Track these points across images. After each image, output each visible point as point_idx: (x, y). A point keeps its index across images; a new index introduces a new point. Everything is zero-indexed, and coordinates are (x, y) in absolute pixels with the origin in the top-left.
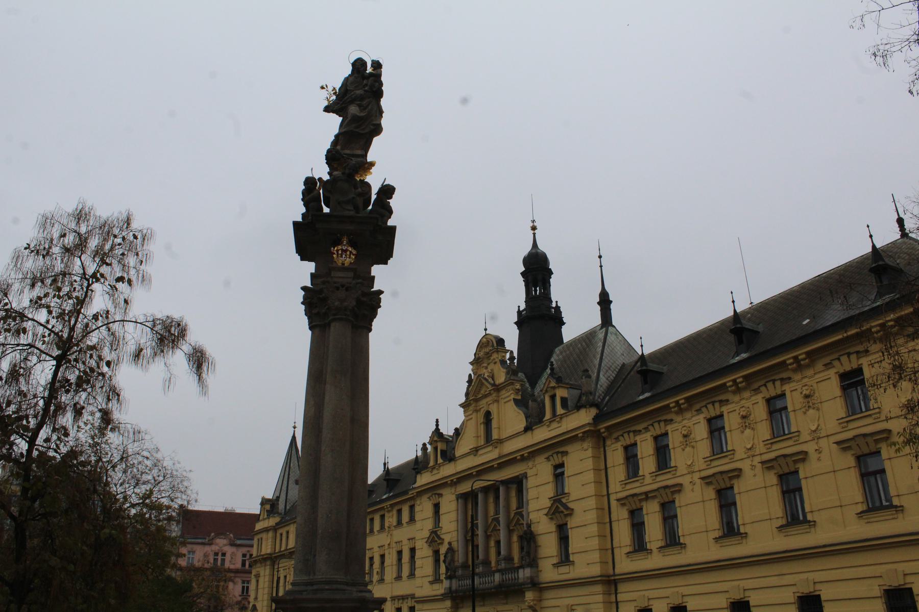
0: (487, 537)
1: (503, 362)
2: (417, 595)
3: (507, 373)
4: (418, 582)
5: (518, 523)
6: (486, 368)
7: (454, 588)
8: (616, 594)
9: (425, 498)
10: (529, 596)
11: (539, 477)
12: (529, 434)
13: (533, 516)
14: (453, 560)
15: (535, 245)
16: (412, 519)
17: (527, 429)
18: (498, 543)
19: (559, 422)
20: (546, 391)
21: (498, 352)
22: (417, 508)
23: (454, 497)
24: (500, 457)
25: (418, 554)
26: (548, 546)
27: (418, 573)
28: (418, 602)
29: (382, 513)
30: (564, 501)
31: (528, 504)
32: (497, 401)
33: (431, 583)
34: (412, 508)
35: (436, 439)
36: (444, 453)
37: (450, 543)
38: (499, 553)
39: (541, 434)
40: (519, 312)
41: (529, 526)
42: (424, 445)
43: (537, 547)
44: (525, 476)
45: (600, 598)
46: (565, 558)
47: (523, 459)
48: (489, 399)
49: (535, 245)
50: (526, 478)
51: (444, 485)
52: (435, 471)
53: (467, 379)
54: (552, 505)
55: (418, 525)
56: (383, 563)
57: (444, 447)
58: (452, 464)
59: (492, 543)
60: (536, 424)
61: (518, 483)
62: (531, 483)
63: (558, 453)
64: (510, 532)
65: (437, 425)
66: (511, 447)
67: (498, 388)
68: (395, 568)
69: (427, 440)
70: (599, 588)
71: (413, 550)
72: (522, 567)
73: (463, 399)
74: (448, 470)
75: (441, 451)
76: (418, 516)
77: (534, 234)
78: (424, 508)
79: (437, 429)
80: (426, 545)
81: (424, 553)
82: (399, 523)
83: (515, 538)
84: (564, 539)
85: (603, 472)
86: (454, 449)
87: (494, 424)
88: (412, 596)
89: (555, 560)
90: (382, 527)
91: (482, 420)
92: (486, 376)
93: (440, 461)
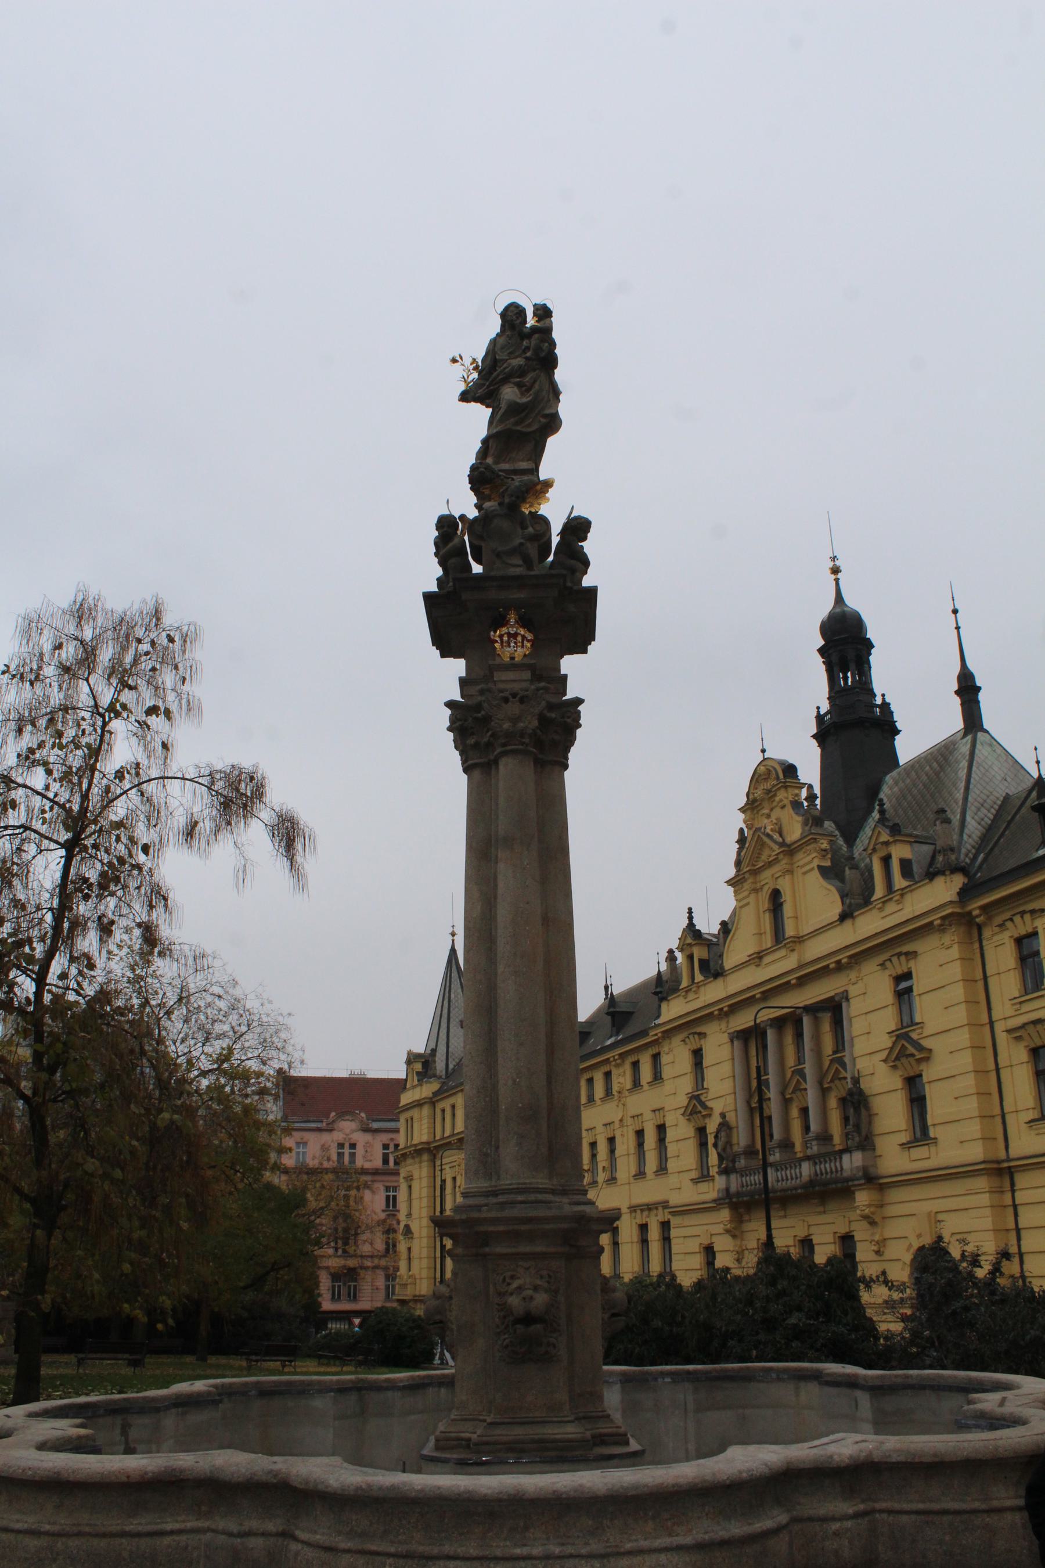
0: (786, 1102)
1: (796, 805)
2: (672, 1203)
3: (805, 823)
4: (672, 1180)
5: (836, 1077)
6: (768, 816)
8: (1013, 1191)
10: (863, 1198)
13: (862, 1064)
14: (729, 1143)
16: (657, 1077)
17: (844, 917)
18: (805, 1111)
21: (786, 787)
22: (665, 1059)
24: (801, 967)
25: (671, 1135)
27: (671, 1165)
29: (606, 1068)
31: (852, 1046)
32: (790, 872)
33: (695, 1181)
34: (656, 1057)
35: (689, 941)
36: (704, 965)
38: (807, 1128)
41: (856, 1081)
42: (671, 952)
43: (871, 1116)
44: (845, 996)
45: (985, 1199)
46: (921, 1133)
48: (776, 869)
50: (847, 999)
51: (709, 1017)
52: (691, 996)
55: (668, 1086)
56: (612, 1151)
57: (705, 955)
59: (795, 1112)
61: (834, 1009)
62: (854, 1009)
64: (824, 1092)
65: (690, 918)
67: (790, 850)
68: (633, 1161)
69: (674, 944)
70: (982, 1183)
71: (661, 1129)
72: (847, 1150)
74: (714, 992)
76: (667, 1072)
79: (691, 925)
80: (682, 1121)
81: (680, 1132)
82: (636, 1084)
83: (833, 1103)
86: (721, 956)
89: (904, 1138)
90: (608, 1092)
91: (766, 906)
92: (768, 830)
93: (699, 977)
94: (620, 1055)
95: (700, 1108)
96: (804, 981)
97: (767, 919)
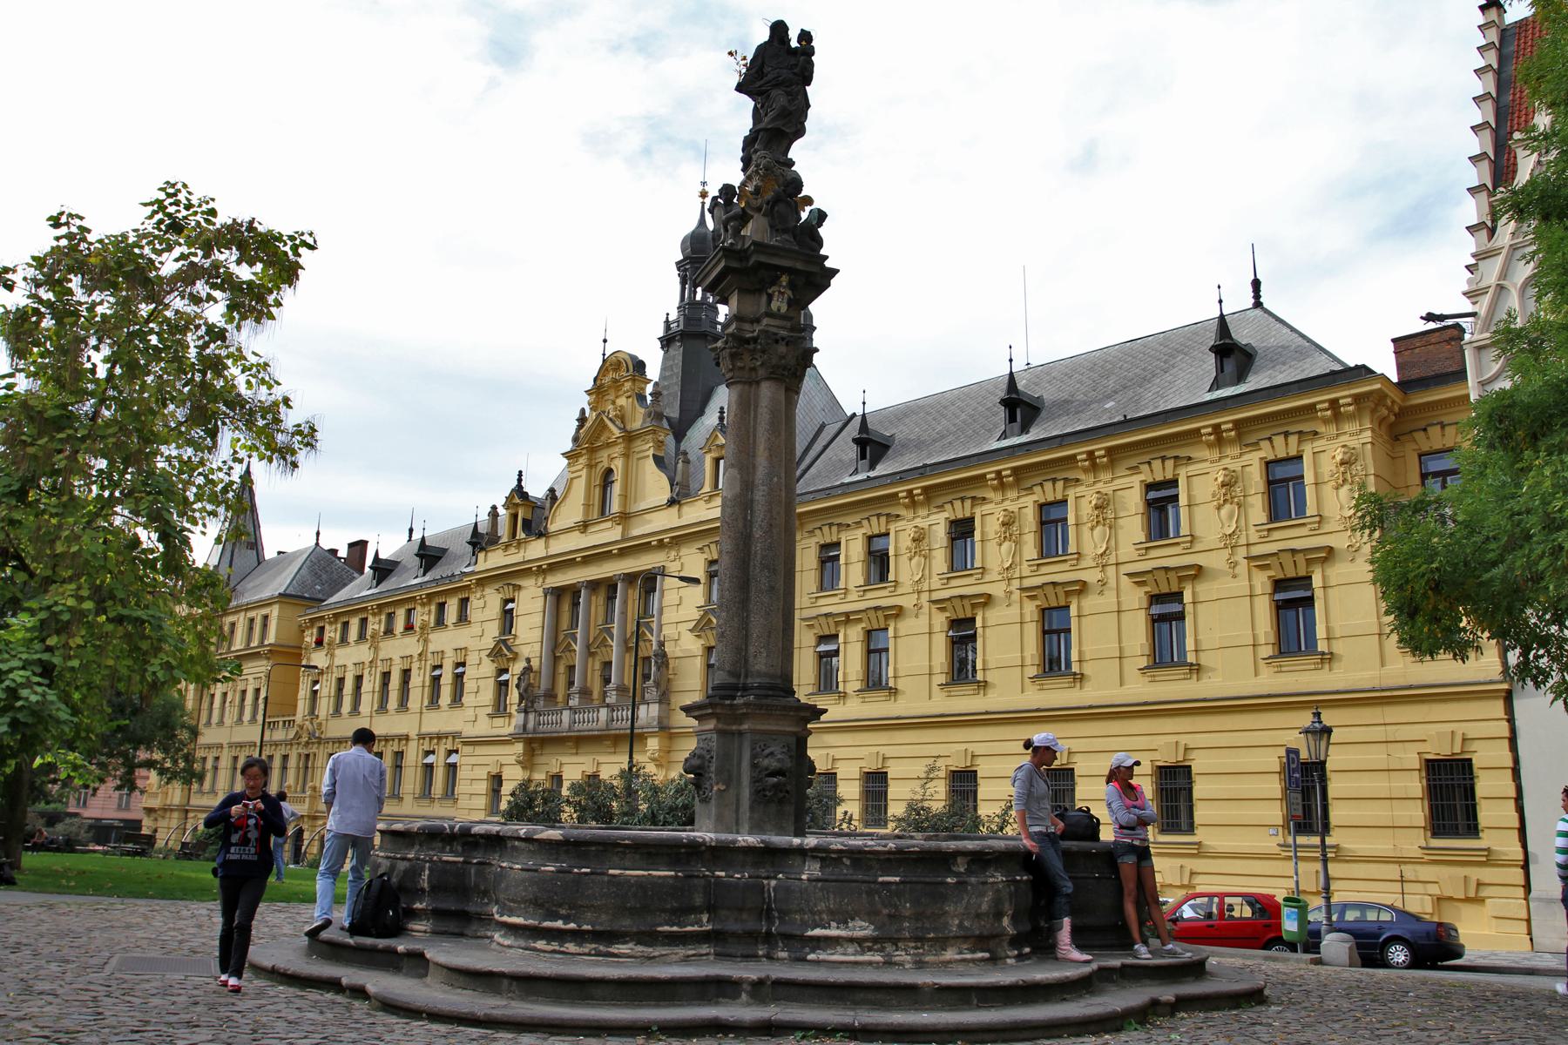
0: (589, 653)
12: (675, 509)
16: (463, 618)
17: (672, 502)
25: (470, 672)
28: (465, 743)
31: (661, 612)
34: (464, 602)
36: (527, 525)
41: (661, 644)
47: (661, 545)
51: (526, 573)
53: (577, 415)
54: (702, 617)
57: (529, 517)
58: (542, 541)
61: (648, 582)
65: (520, 480)
69: (500, 502)
73: (568, 446)
74: (536, 550)
75: (524, 520)
88: (455, 736)
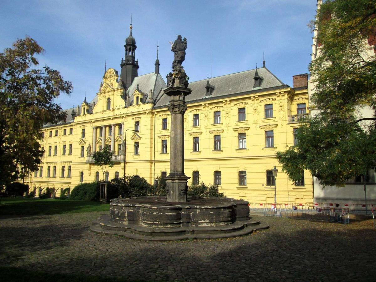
7: (90, 161)
9: (78, 126)
11: (129, 124)
12: (126, 108)
15: (131, 35)
17: (125, 107)
19: (139, 107)
20: (135, 95)
22: (73, 130)
23: (92, 128)
26: (130, 148)
29: (56, 130)
30: (138, 134)
33: (80, 158)
36: (88, 111)
37: (89, 144)
39: (131, 109)
40: (122, 61)
48: (110, 93)
49: (131, 35)
57: (88, 108)
58: (92, 115)
60: (129, 106)
63: (137, 117)
65: (85, 99)
66: (117, 112)
71: (71, 145)
74: (89, 117)
75: (87, 110)
77: (131, 31)
78: (77, 130)
79: (85, 102)
84: (137, 145)
85: (153, 126)
87: (112, 103)
94: (61, 127)
95: (83, 142)
96: (113, 119)
97: (106, 104)
